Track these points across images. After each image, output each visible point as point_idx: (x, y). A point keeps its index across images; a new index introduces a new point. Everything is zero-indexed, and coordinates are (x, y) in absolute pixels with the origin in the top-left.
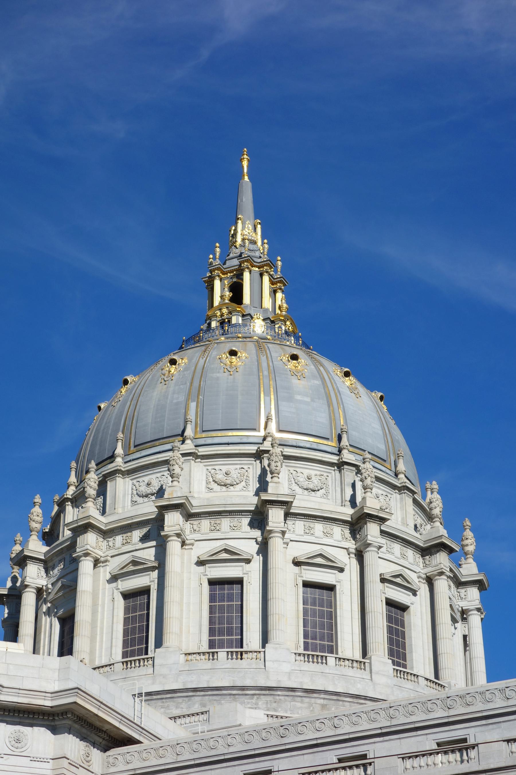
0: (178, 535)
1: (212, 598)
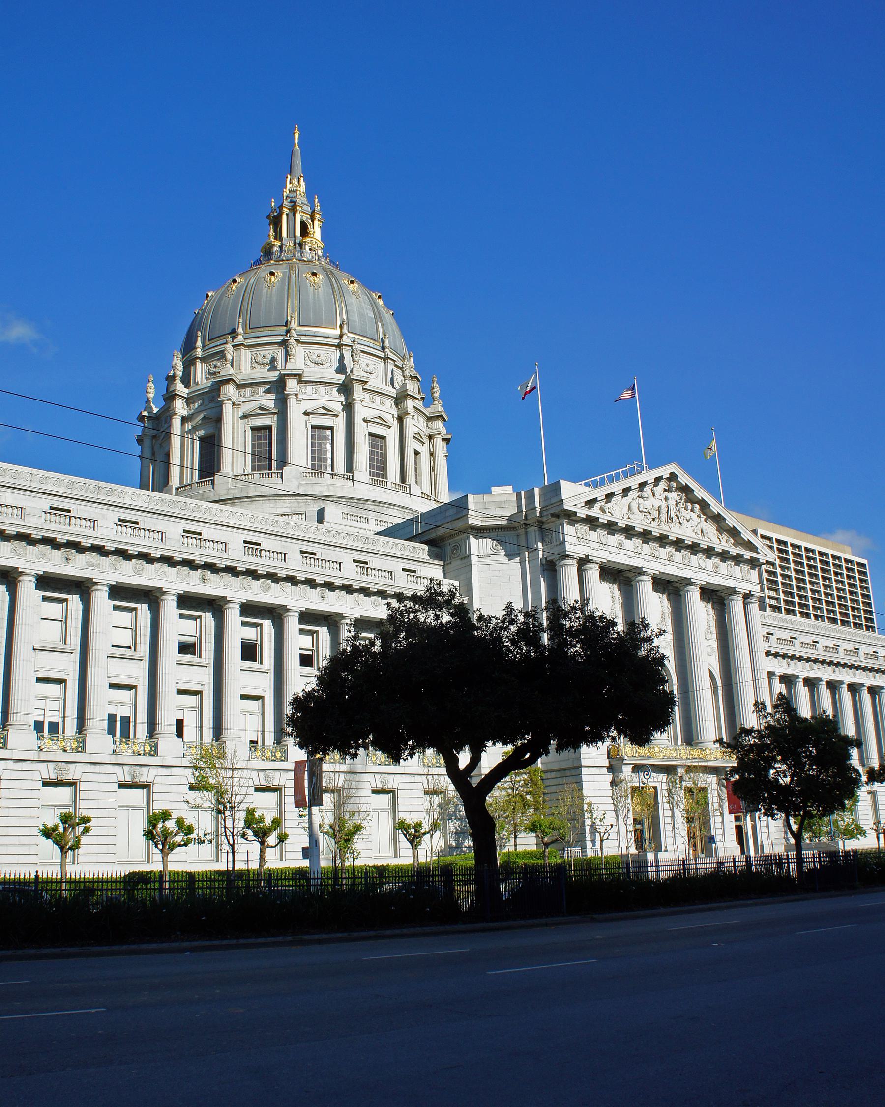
0: (296, 395)
1: (313, 437)
